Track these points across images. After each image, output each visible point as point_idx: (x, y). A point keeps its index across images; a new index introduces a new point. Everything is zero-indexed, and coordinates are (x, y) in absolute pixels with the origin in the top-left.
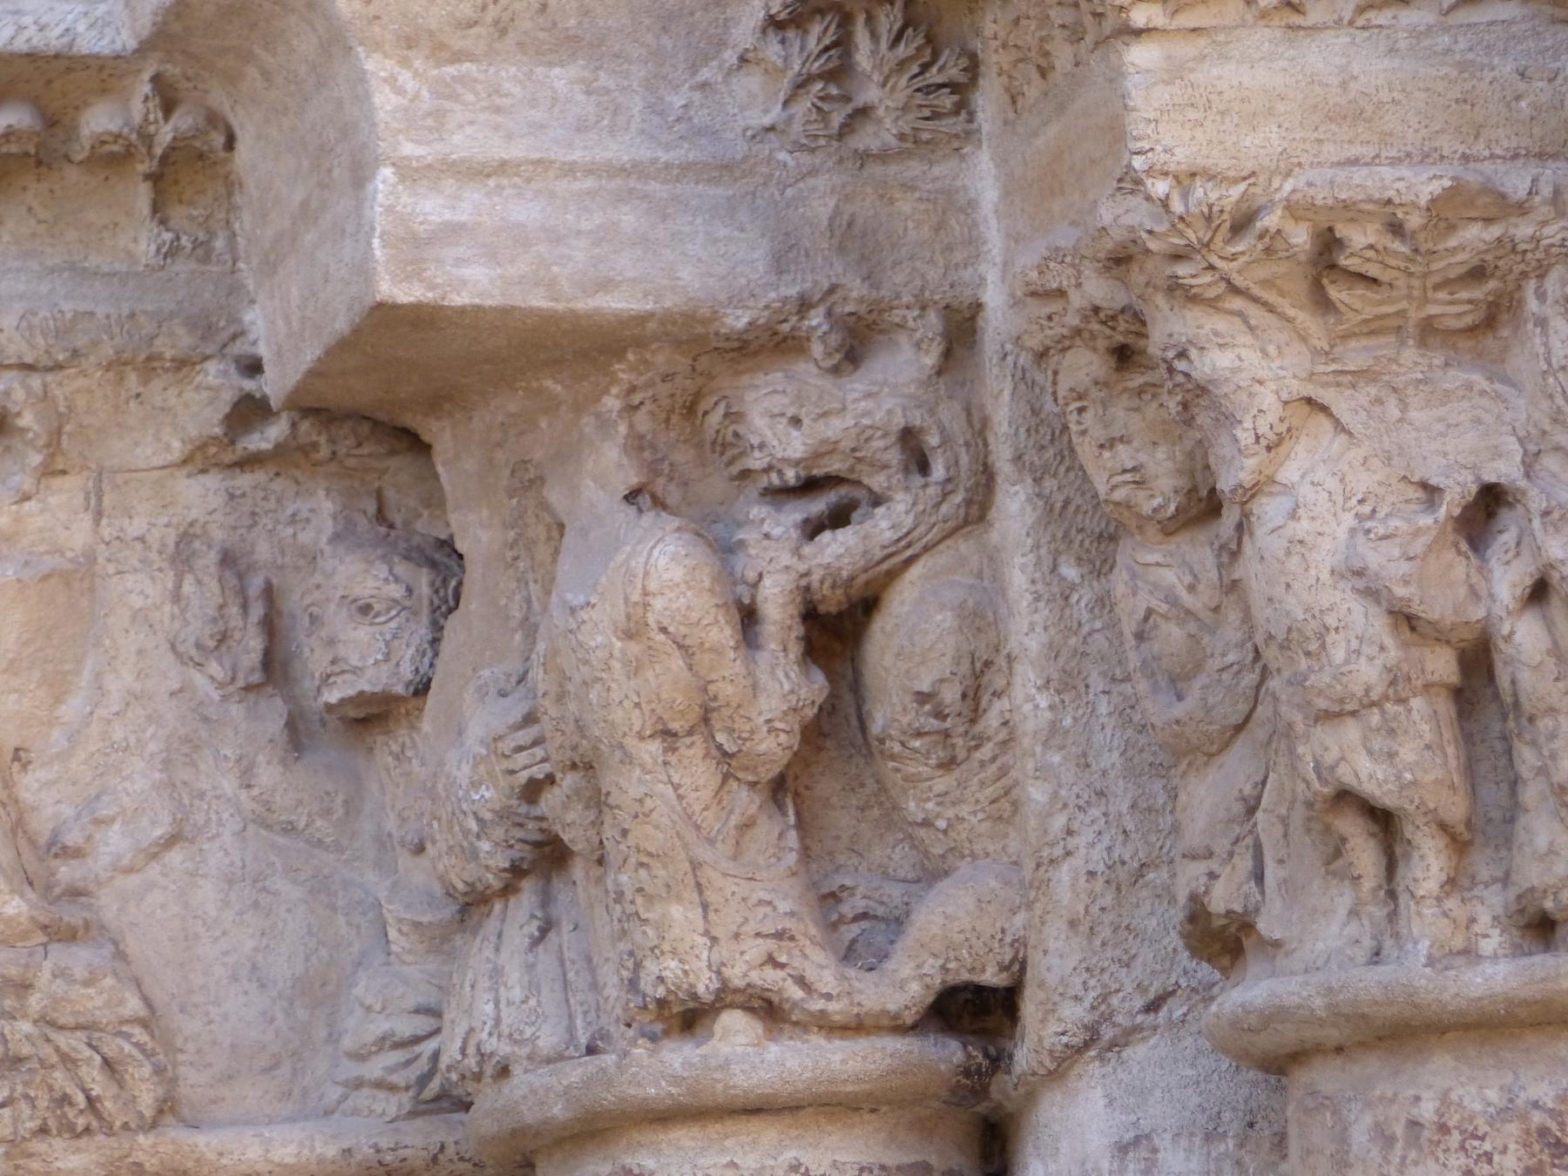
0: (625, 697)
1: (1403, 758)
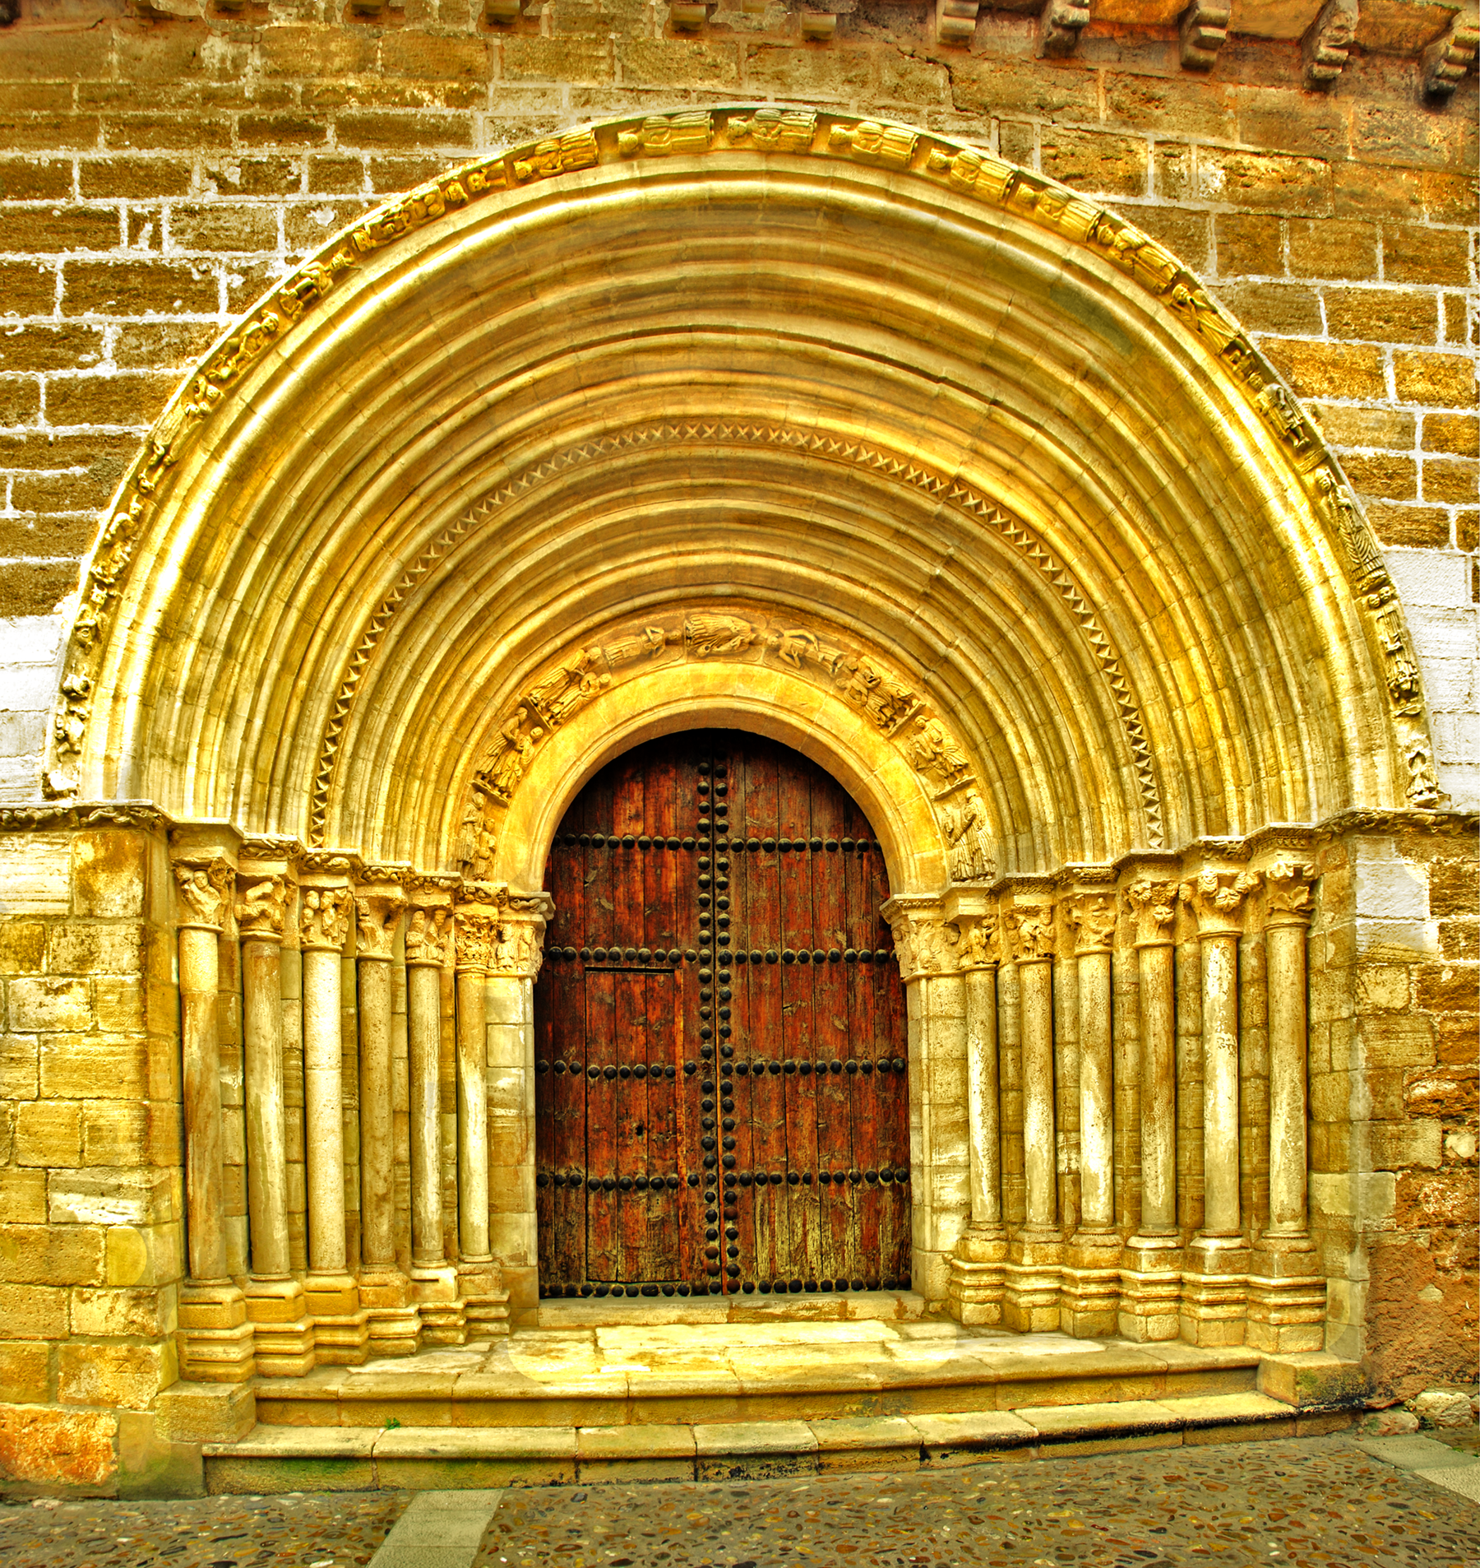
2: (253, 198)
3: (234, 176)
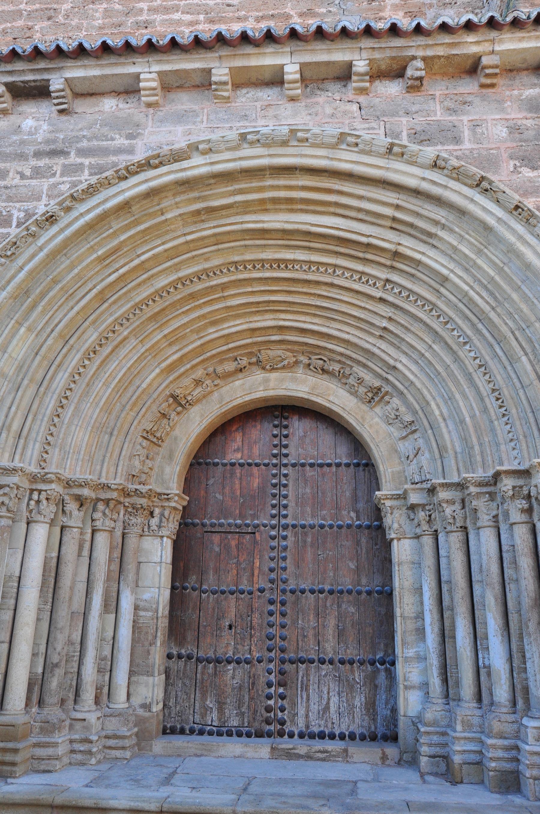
0: (421, 519)
1: (451, 521)
2: (35, 181)
3: (28, 172)
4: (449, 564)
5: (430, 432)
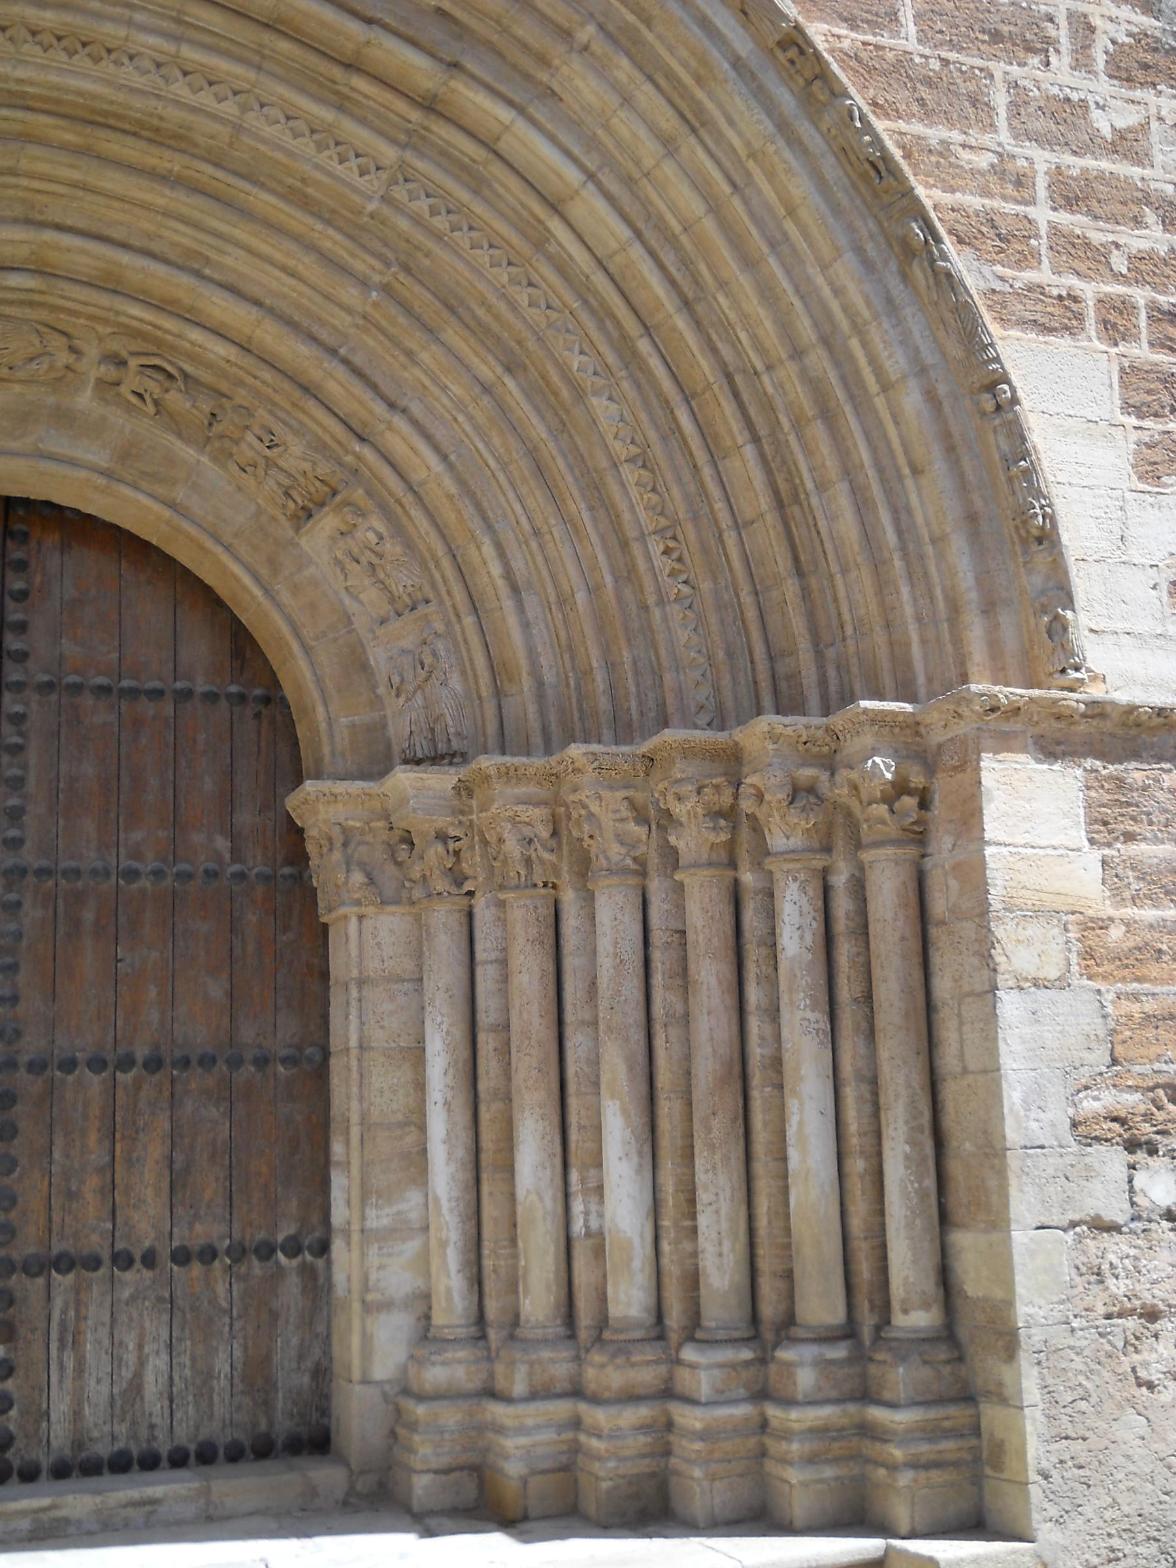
4: (505, 979)
5: (469, 620)
